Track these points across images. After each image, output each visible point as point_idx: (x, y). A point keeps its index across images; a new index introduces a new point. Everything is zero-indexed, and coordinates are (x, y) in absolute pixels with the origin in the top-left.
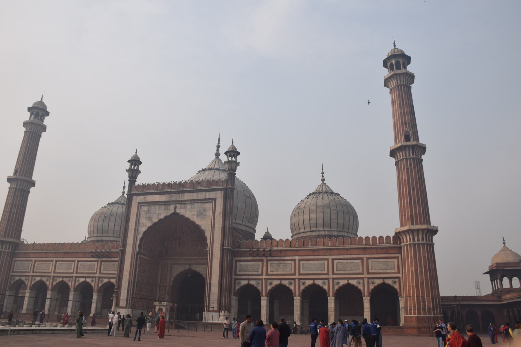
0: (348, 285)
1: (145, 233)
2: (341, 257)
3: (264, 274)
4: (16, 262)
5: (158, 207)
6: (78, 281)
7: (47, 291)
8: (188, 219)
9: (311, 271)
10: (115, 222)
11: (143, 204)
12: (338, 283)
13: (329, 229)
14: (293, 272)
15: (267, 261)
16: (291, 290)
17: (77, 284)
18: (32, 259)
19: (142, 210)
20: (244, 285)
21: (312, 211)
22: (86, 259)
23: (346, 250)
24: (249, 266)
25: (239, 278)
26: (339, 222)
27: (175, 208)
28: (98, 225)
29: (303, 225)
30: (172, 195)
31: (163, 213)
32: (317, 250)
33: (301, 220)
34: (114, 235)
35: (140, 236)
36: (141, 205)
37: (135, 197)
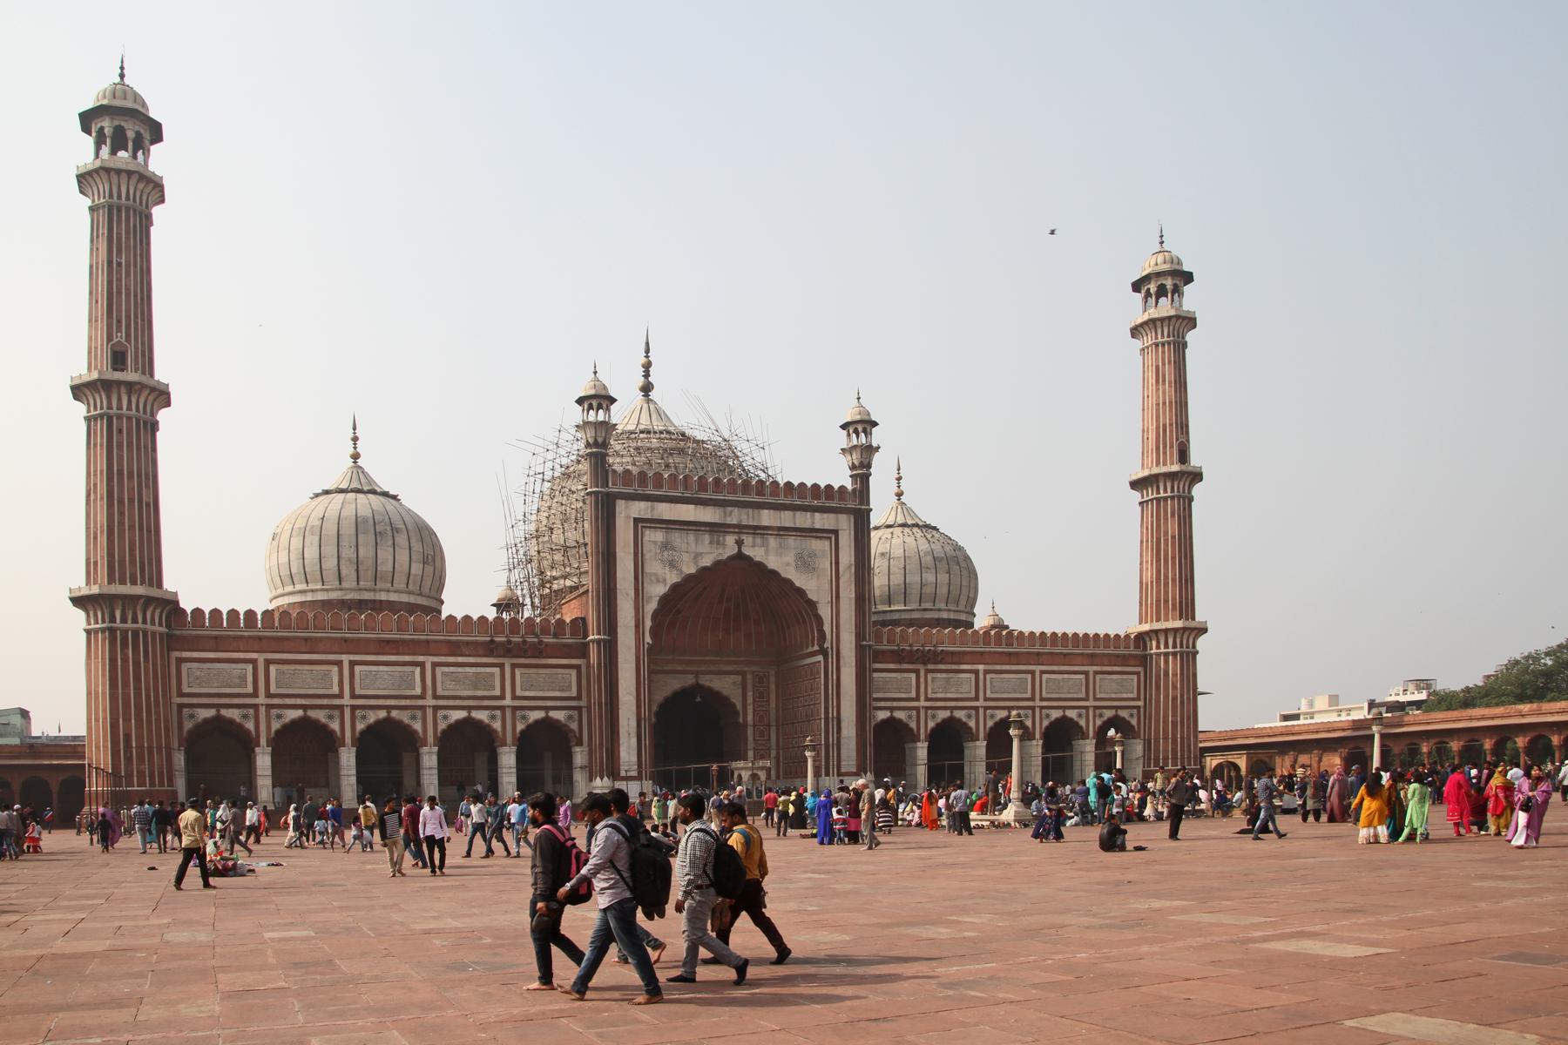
2: (1055, 668)
3: (922, 698)
4: (185, 667)
6: (445, 717)
10: (410, 549)
13: (956, 609)
15: (927, 671)
18: (254, 656)
20: (883, 721)
21: (927, 568)
22: (461, 659)
23: (1062, 656)
28: (360, 556)
29: (903, 596)
32: (1017, 654)
33: (899, 585)
37: (623, 501)
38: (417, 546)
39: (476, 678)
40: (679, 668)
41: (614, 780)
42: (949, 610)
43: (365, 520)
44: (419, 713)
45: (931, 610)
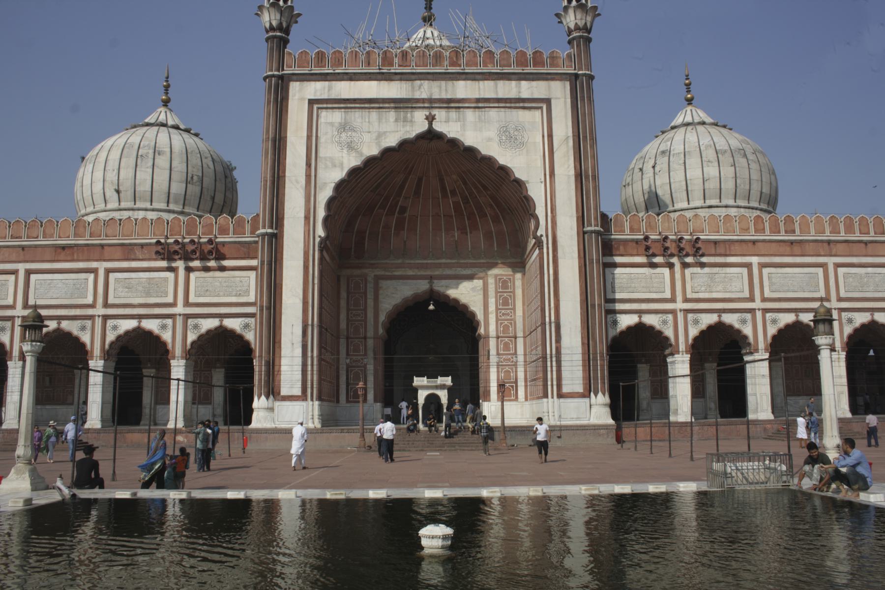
0: (873, 323)
1: (340, 186)
2: (854, 260)
3: (679, 298)
5: (374, 114)
6: (115, 328)
7: (7, 361)
8: (471, 152)
9: (788, 291)
10: (171, 170)
11: (325, 106)
12: (850, 321)
13: (747, 205)
14: (746, 294)
15: (685, 265)
16: (746, 337)
17: (111, 337)
19: (322, 120)
20: (630, 329)
21: (709, 161)
23: (863, 245)
24: (638, 278)
25: (623, 310)
26: (764, 191)
27: (431, 119)
28: (120, 178)
29: (685, 193)
30: (418, 82)
31: (393, 132)
32: (800, 242)
33: (680, 181)
34: (168, 206)
35: (325, 194)
36: (318, 108)
38: (179, 166)
39: (149, 284)
40: (410, 273)
41: (275, 399)
42: (738, 207)
43: (132, 146)
44: (89, 323)
45: (717, 207)
